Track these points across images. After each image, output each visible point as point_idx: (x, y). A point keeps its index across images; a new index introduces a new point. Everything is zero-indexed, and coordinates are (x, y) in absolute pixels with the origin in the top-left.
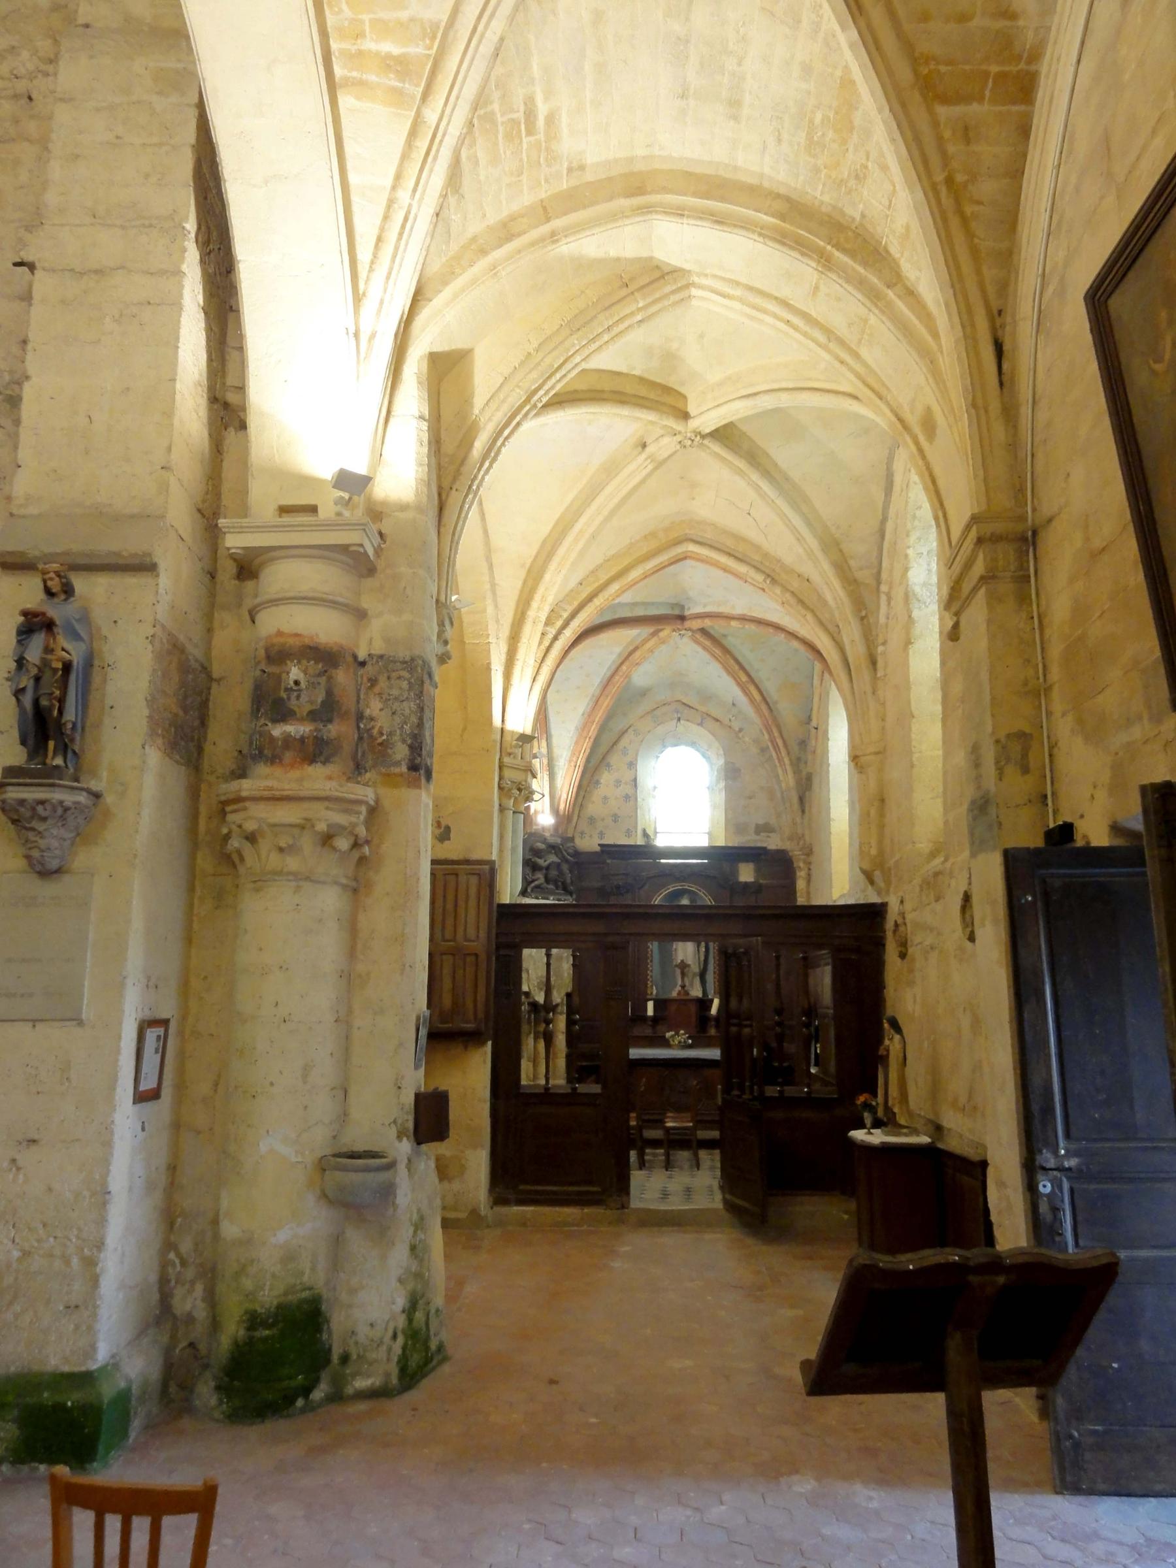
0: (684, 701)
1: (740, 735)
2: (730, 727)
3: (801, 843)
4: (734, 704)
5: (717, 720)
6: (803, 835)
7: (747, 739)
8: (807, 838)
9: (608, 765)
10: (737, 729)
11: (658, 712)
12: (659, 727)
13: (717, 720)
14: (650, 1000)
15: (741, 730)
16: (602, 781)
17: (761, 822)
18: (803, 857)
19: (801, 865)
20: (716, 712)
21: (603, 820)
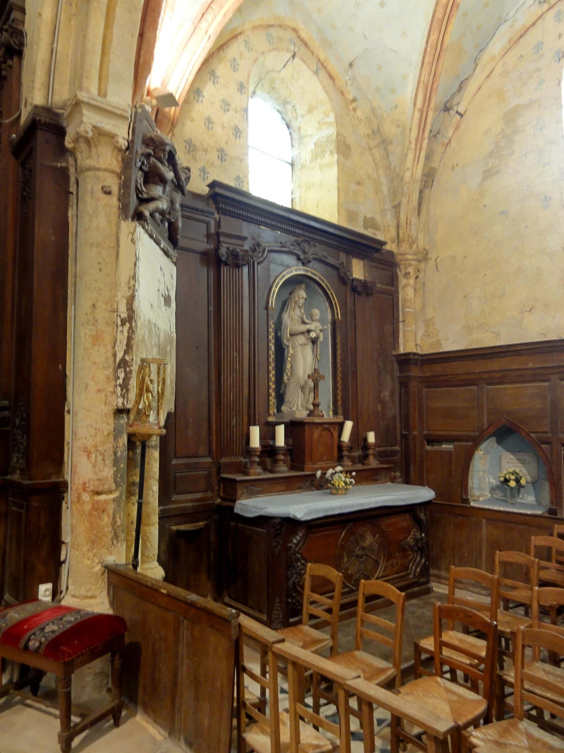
0: (303, 35)
1: (354, 105)
2: (342, 93)
3: (414, 246)
4: (351, 65)
5: (331, 77)
6: (417, 238)
7: (359, 113)
8: (421, 243)
9: (213, 73)
10: (351, 98)
11: (272, 31)
12: (274, 53)
13: (331, 77)
14: (279, 423)
15: (354, 100)
16: (205, 93)
17: (369, 216)
18: (413, 263)
19: (411, 270)
20: (334, 66)
21: (206, 151)
